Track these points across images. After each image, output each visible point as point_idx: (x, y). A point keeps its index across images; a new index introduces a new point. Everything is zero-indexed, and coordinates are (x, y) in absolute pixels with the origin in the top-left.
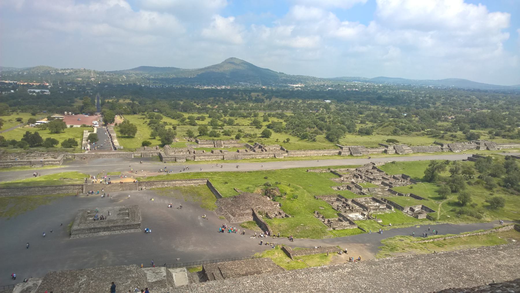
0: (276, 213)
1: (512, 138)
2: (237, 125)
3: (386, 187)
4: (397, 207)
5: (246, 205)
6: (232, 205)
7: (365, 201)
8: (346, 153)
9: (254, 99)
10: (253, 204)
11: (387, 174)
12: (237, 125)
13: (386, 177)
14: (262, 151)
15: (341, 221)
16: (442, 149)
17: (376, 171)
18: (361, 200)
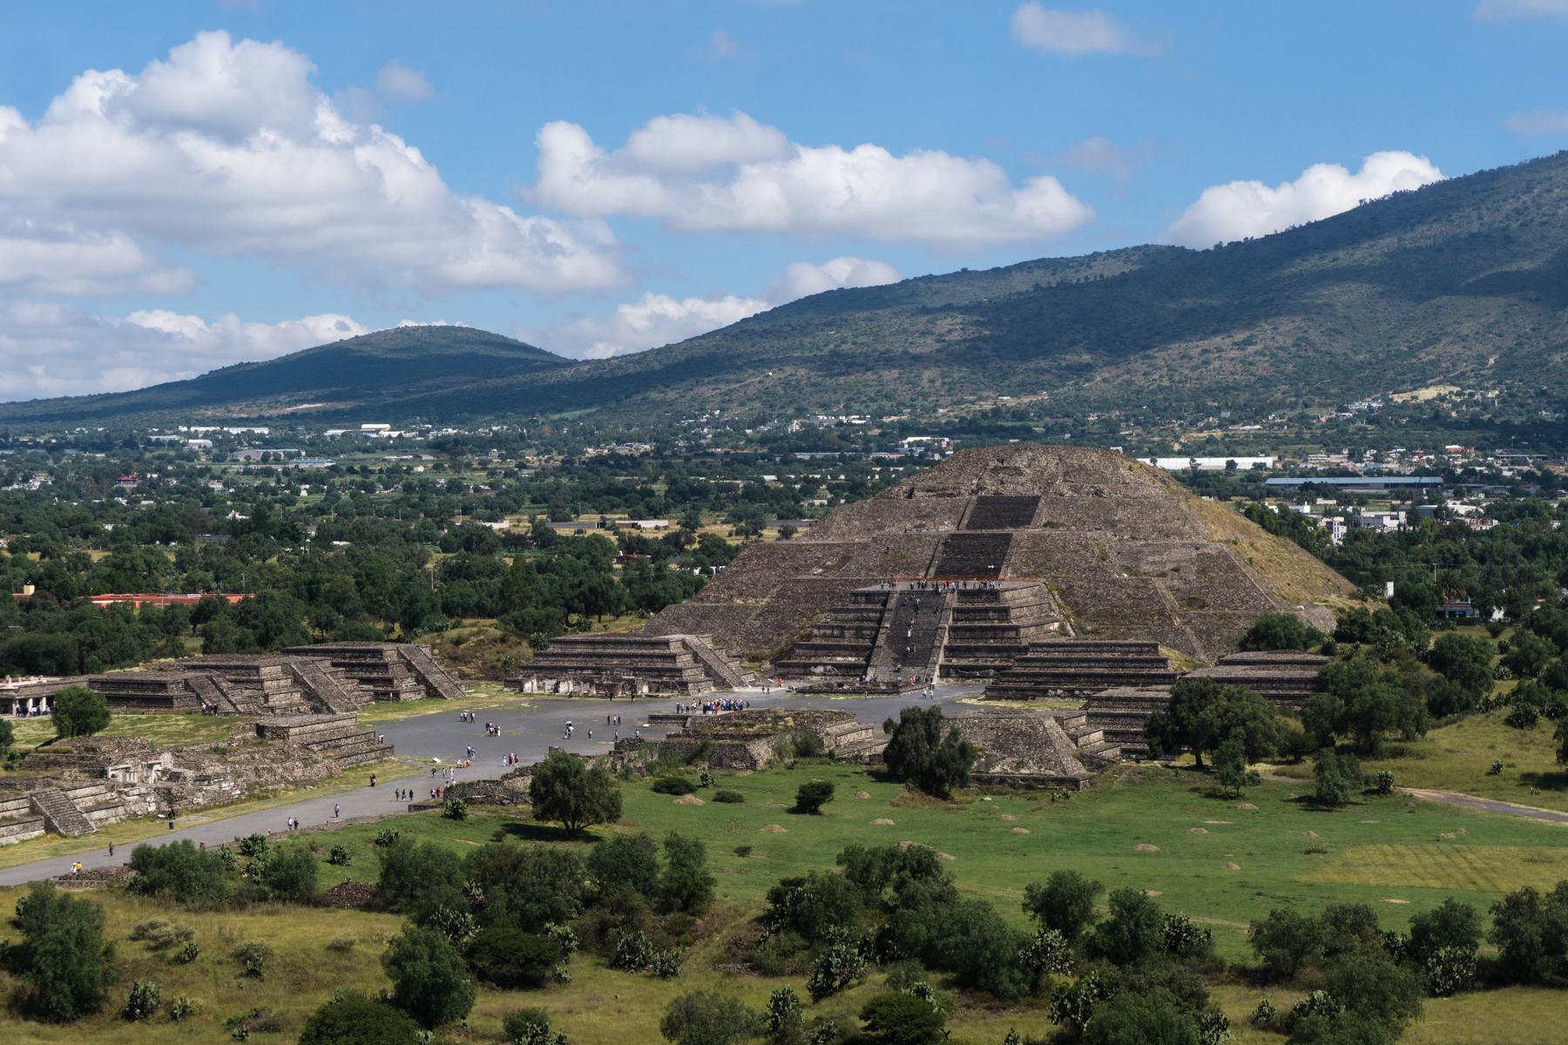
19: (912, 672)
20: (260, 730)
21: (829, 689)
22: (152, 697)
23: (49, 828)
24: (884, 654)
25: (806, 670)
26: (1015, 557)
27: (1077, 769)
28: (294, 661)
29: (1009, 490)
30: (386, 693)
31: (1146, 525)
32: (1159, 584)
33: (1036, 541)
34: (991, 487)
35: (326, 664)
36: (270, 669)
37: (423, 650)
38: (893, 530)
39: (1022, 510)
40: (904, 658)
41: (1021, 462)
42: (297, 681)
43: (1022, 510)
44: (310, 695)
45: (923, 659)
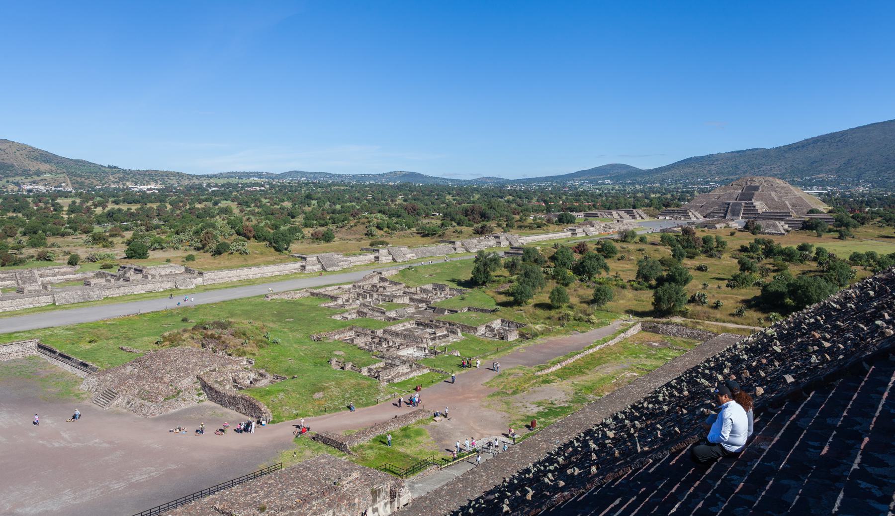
0: (252, 375)
2: (53, 245)
3: (420, 305)
4: (466, 328)
5: (178, 371)
6: (139, 378)
7: (405, 330)
8: (314, 267)
9: (66, 208)
10: (196, 364)
11: (408, 287)
12: (53, 245)
13: (408, 290)
14: (146, 277)
15: (392, 366)
16: (455, 249)
17: (386, 284)
18: (398, 328)
22: (595, 216)
26: (755, 197)
30: (634, 217)
33: (759, 194)
34: (749, 184)
36: (614, 212)
37: (640, 211)
39: (756, 188)
40: (733, 215)
41: (755, 179)
43: (756, 188)
45: (738, 215)
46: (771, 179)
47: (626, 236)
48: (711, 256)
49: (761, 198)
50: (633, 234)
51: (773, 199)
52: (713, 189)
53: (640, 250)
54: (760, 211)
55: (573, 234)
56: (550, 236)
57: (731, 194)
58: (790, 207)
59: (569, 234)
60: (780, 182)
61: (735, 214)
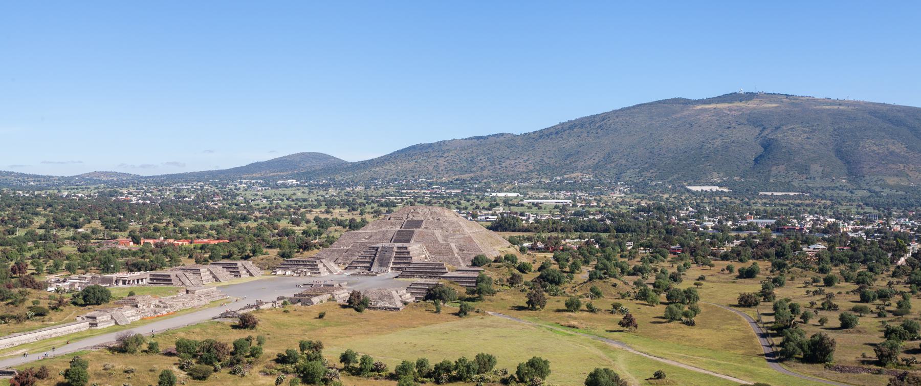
1: (18, 319)
19: (383, 269)
20: (187, 292)
21: (359, 274)
23: (116, 323)
24: (376, 264)
25: (356, 268)
27: (399, 305)
28: (211, 267)
29: (415, 219)
30: (237, 274)
31: (450, 228)
32: (453, 245)
33: (421, 233)
34: (411, 216)
35: (221, 267)
36: (204, 270)
37: (249, 264)
38: (384, 229)
39: (418, 224)
40: (381, 265)
41: (419, 210)
42: (211, 273)
43: (418, 224)
44: (214, 277)
45: (386, 265)
46: (437, 209)
47: (127, 344)
48: (233, 373)
49: (423, 239)
50: (138, 340)
51: (436, 241)
52: (364, 223)
53: (126, 372)
54: (415, 260)
55: (92, 325)
56: (45, 333)
57: (385, 233)
58: (456, 250)
59: (84, 325)
60: (450, 214)
61: (383, 263)
